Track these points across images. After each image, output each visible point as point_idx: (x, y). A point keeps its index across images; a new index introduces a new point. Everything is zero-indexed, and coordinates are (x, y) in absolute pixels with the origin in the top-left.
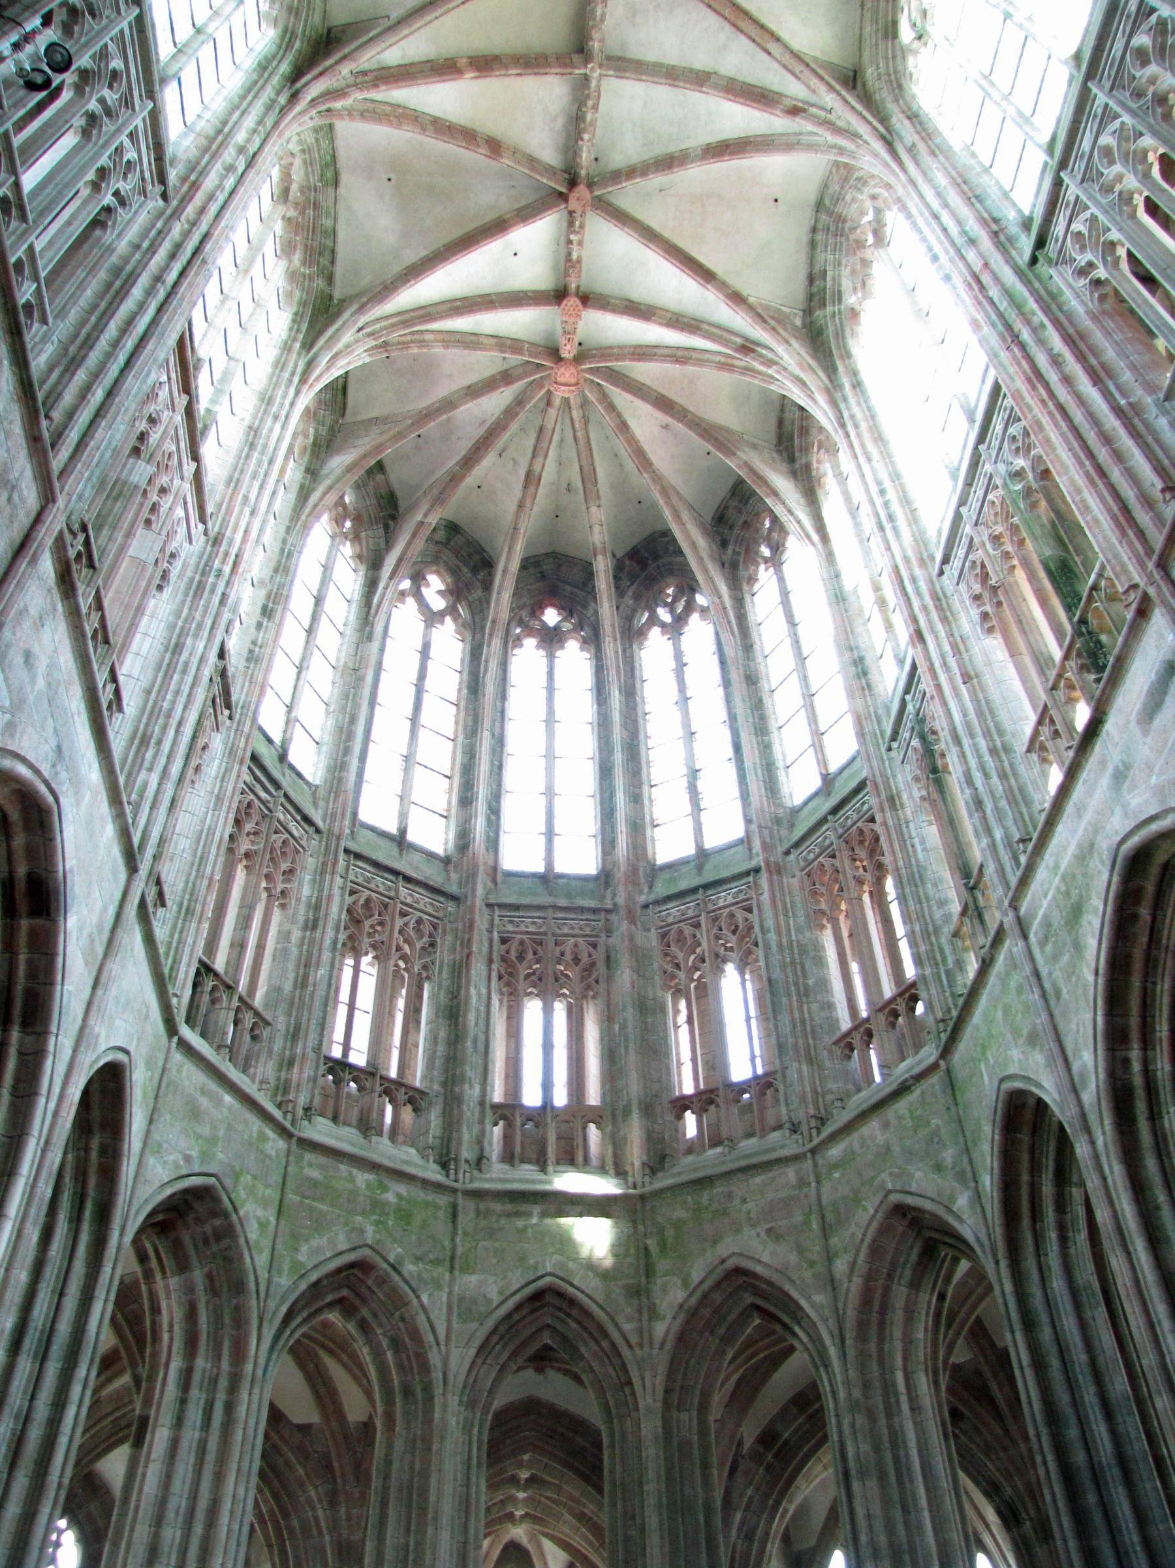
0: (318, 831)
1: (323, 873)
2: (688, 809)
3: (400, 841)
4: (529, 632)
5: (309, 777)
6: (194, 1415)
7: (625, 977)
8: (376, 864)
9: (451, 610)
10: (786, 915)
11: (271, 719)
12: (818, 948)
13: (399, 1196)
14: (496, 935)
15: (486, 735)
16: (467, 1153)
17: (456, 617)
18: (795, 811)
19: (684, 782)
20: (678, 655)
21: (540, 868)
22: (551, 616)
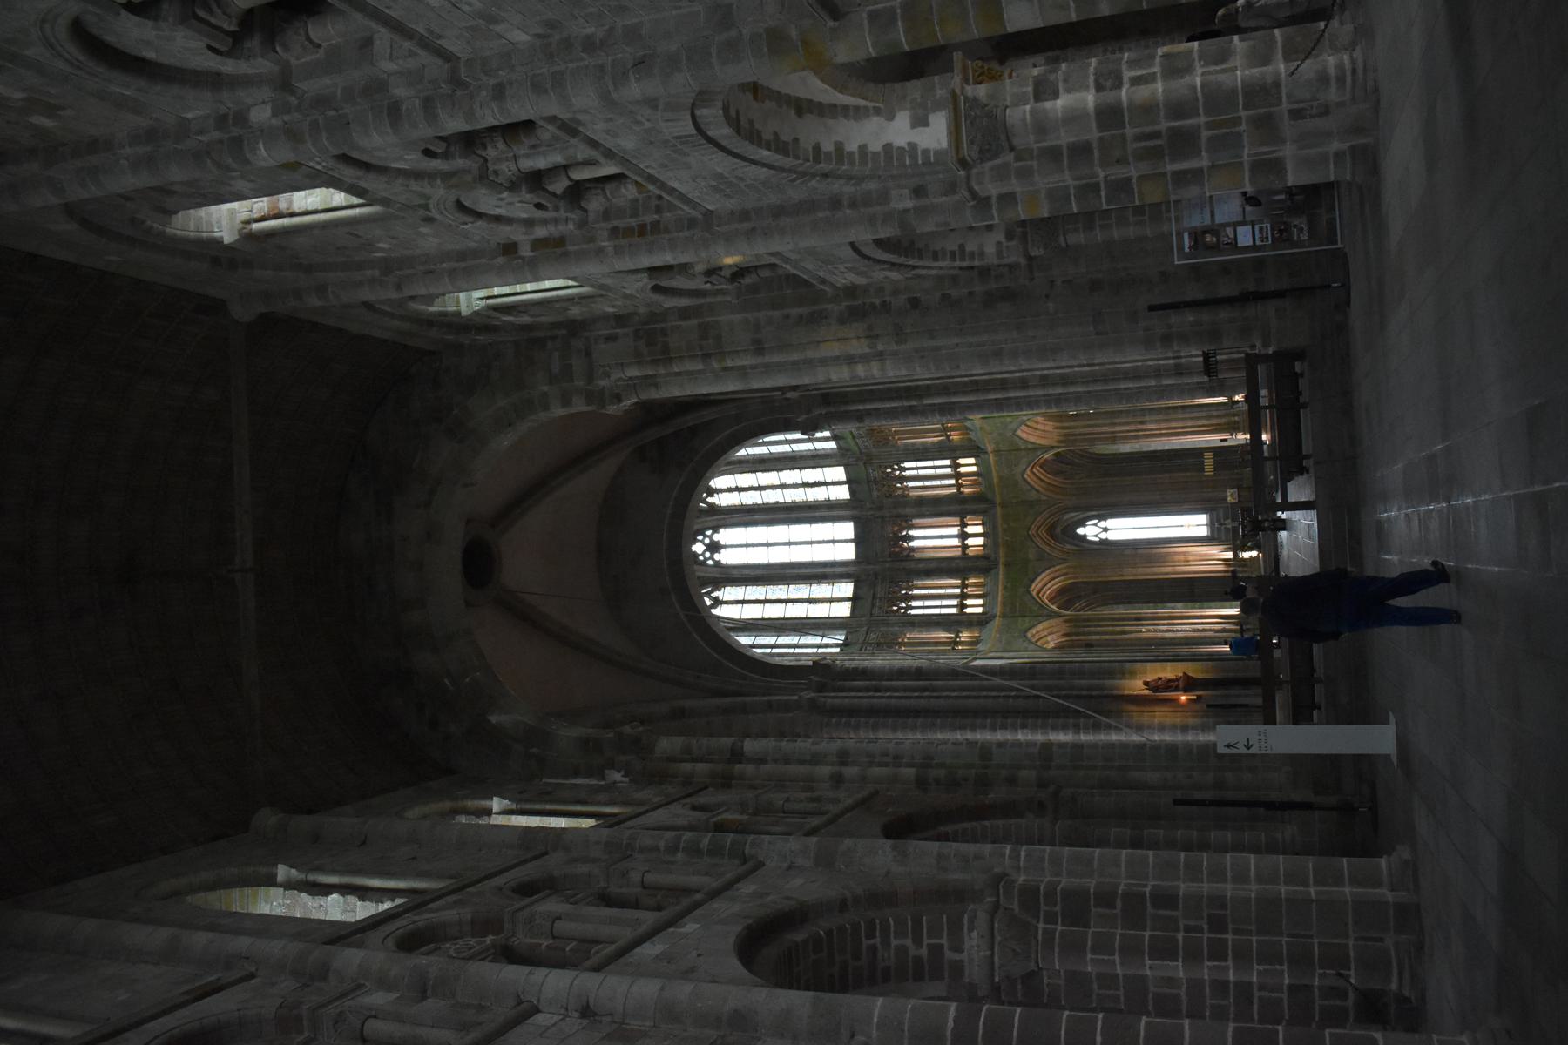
0: (868, 629)
1: (888, 624)
2: (824, 488)
3: (855, 600)
4: (711, 558)
5: (843, 637)
6: (1087, 629)
7: (908, 511)
8: (873, 605)
9: (708, 594)
10: (891, 455)
11: (837, 650)
12: (906, 444)
13: (1007, 582)
14: (889, 559)
15: (787, 571)
16: (985, 563)
17: (712, 591)
18: (839, 447)
19: (808, 490)
20: (730, 490)
21: (852, 545)
22: (698, 548)
